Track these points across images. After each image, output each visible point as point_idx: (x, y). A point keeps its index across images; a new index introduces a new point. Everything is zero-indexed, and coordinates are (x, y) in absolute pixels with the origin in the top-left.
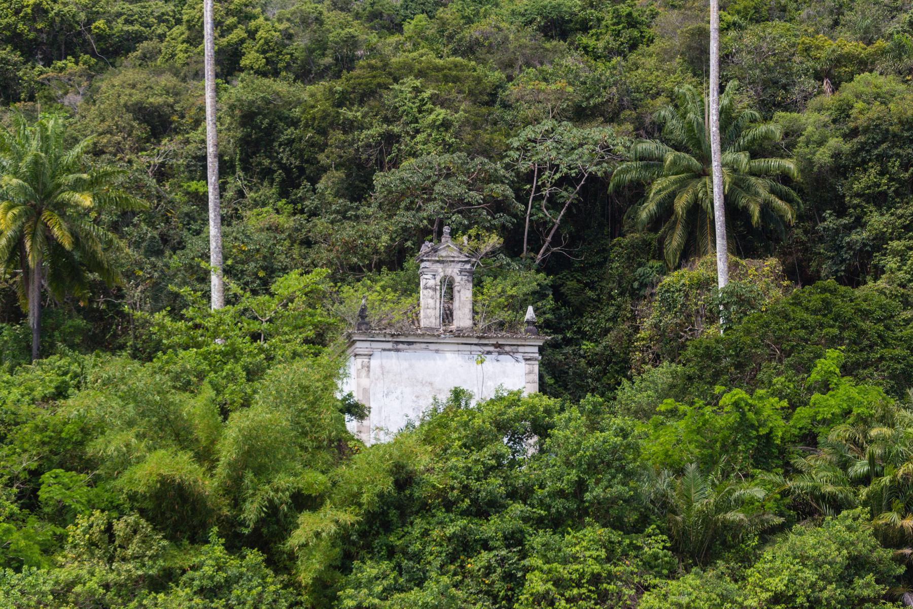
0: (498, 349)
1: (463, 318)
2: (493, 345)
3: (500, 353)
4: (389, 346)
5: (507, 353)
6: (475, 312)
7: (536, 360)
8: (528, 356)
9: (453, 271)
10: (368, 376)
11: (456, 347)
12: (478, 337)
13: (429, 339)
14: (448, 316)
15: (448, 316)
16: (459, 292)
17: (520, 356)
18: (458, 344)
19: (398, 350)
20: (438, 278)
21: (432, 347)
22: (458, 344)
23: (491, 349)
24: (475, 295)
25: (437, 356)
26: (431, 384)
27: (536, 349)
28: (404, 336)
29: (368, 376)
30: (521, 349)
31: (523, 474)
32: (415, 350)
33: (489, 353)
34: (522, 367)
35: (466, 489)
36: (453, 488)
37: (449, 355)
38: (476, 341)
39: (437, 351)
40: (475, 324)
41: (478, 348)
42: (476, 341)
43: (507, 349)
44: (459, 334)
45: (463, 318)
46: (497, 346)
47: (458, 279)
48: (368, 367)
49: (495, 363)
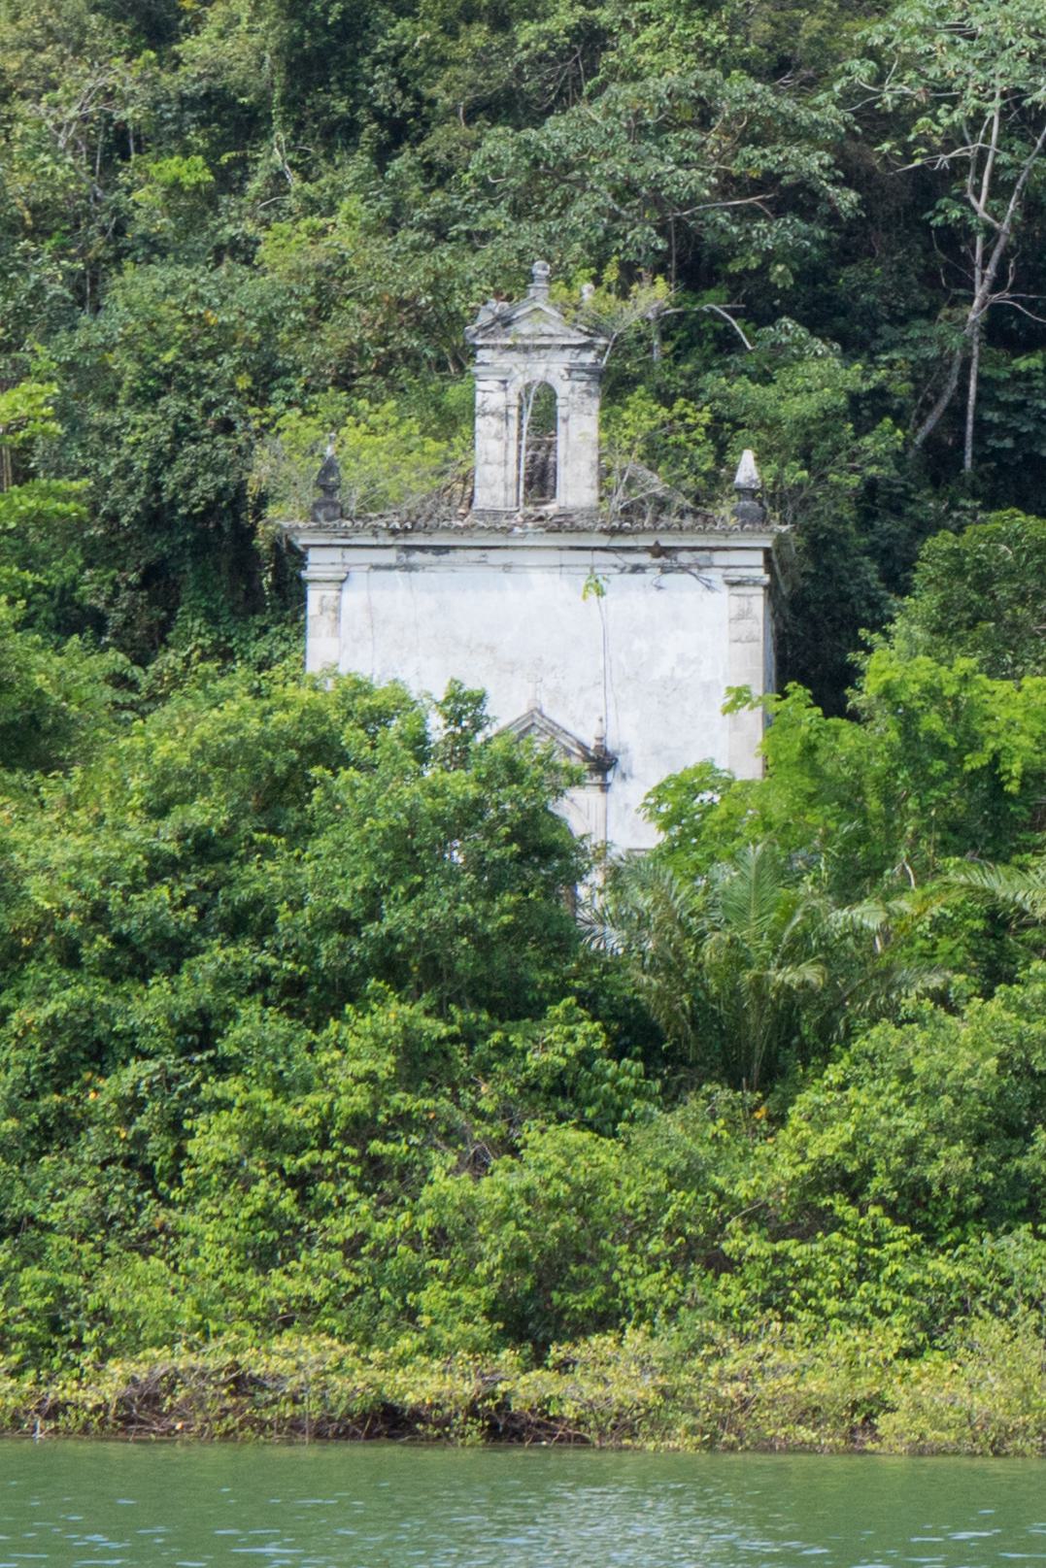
0: (662, 560)
1: (576, 488)
2: (648, 549)
3: (665, 570)
4: (390, 557)
5: (684, 569)
6: (605, 473)
7: (755, 584)
8: (735, 575)
9: (552, 369)
10: (335, 631)
11: (555, 557)
12: (603, 531)
13: (491, 538)
14: (540, 479)
15: (540, 479)
16: (565, 420)
17: (715, 576)
18: (561, 549)
19: (409, 568)
20: (514, 389)
21: (494, 556)
22: (561, 549)
23: (645, 559)
24: (605, 424)
25: (507, 579)
26: (491, 649)
27: (758, 558)
28: (427, 530)
29: (335, 631)
30: (719, 558)
31: (261, 877)
32: (453, 567)
33: (637, 569)
34: (722, 603)
35: (98, 914)
36: (65, 911)
37: (537, 577)
38: (604, 541)
39: (507, 567)
40: (601, 499)
41: (611, 558)
42: (604, 541)
43: (684, 558)
44: (561, 525)
45: (576, 488)
46: (659, 551)
47: (562, 388)
48: (337, 610)
49: (654, 593)
